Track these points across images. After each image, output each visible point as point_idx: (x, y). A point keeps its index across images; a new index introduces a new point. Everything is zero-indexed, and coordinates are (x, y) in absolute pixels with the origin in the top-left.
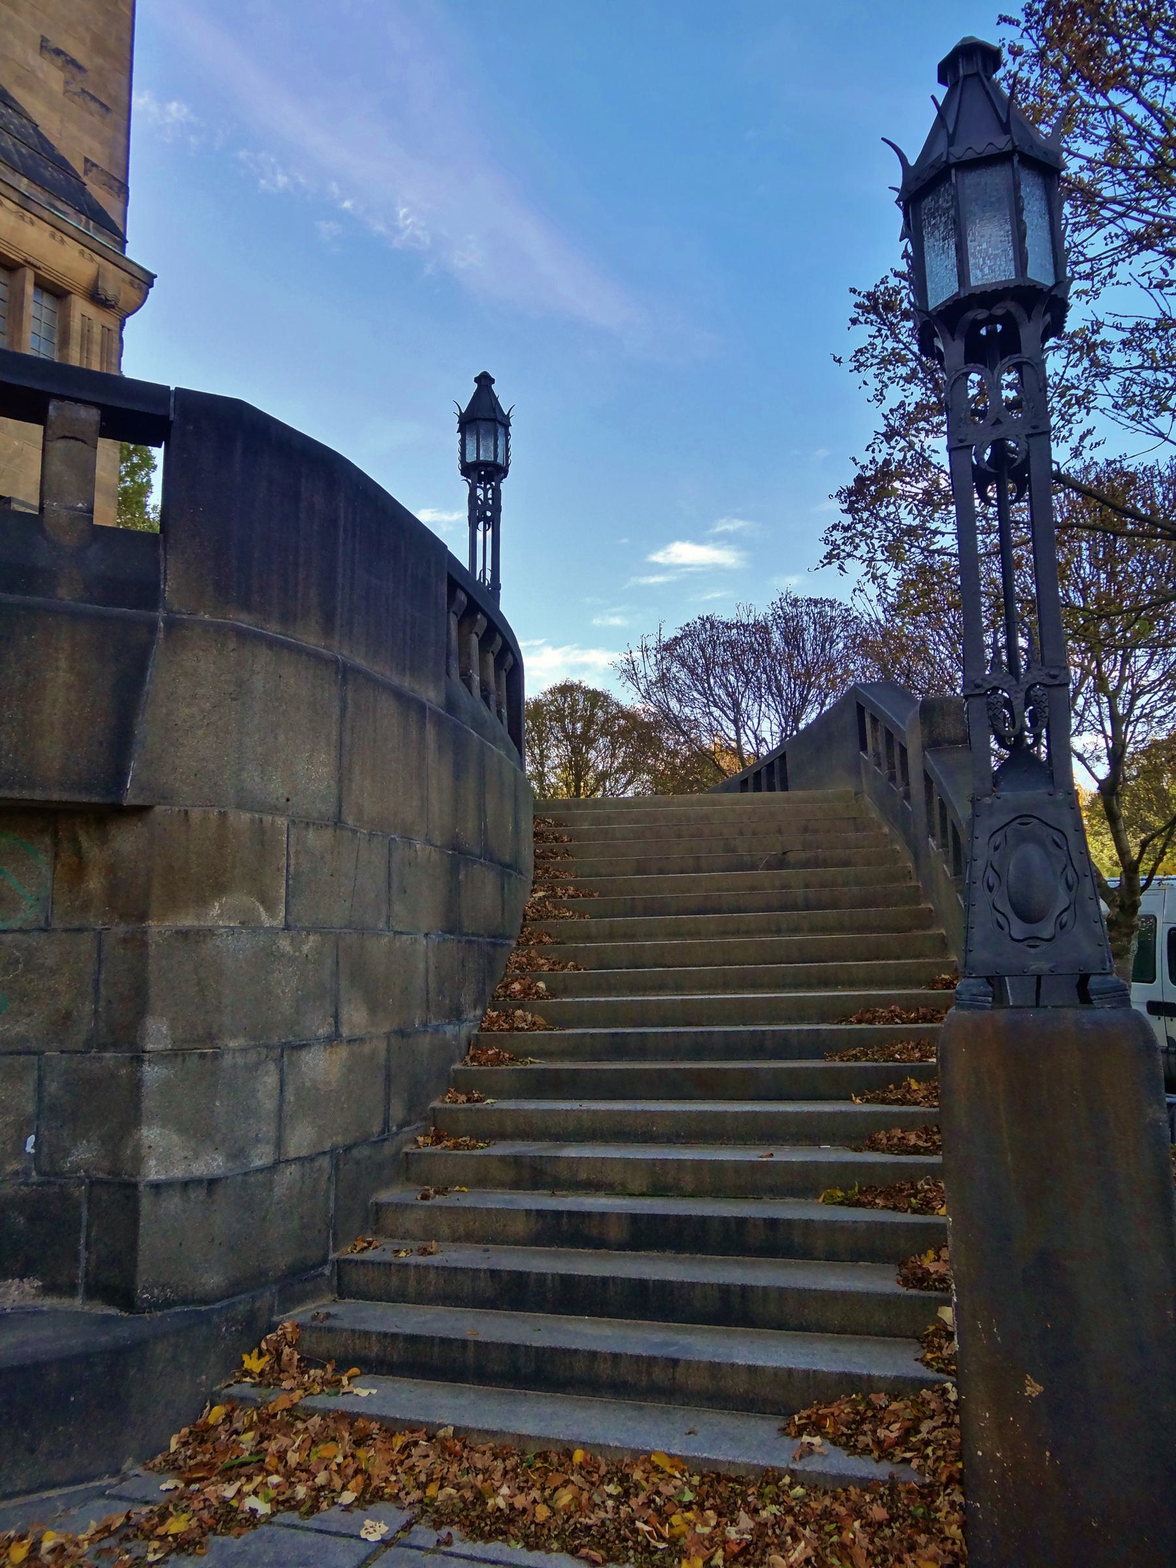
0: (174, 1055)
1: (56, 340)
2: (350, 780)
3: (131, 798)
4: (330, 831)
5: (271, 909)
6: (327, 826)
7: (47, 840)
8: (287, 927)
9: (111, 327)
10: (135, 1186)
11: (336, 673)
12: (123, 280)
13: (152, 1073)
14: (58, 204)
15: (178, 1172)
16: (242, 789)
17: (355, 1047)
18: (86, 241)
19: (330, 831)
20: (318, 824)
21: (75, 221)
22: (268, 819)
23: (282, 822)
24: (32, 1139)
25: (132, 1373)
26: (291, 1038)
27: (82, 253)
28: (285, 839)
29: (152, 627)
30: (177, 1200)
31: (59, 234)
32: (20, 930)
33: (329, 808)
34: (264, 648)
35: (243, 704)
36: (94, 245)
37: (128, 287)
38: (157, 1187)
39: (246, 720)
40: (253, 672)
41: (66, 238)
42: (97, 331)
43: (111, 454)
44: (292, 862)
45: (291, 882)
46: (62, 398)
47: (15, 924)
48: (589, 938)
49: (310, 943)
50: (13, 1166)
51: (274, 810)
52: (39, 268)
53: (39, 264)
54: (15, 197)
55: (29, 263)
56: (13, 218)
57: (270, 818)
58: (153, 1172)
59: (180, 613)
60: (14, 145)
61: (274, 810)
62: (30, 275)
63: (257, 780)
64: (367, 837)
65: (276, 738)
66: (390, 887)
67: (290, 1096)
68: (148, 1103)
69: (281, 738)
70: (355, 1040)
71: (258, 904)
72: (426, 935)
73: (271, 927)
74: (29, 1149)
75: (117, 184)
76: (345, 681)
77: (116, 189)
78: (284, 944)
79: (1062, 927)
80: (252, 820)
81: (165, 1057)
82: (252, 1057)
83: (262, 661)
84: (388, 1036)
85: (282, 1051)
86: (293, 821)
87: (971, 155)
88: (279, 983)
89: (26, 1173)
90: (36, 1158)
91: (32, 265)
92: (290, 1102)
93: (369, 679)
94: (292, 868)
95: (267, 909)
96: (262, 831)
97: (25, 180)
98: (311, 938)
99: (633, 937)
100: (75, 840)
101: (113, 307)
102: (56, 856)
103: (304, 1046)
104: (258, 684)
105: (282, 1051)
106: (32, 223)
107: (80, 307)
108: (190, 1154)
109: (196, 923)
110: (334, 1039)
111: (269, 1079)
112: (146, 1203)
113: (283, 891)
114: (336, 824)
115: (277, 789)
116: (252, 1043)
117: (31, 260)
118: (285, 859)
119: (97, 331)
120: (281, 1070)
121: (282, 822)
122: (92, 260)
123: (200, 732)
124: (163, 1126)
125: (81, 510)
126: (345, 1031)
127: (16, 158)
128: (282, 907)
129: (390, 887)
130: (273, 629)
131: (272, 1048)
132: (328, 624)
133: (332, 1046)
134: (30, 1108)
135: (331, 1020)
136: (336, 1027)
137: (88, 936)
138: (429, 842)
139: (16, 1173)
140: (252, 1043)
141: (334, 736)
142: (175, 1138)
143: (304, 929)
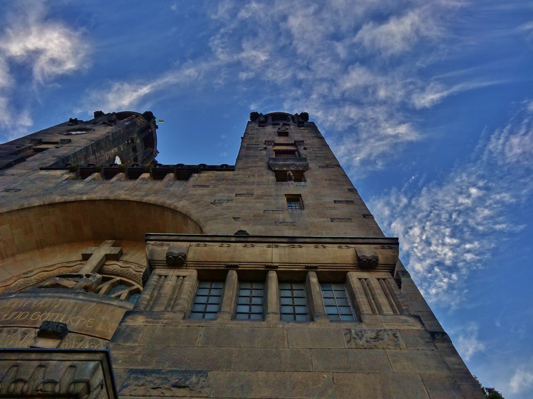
1: (350, 304)
43: (429, 353)
56: (287, 249)
106: (301, 247)
119: (374, 283)
122: (349, 248)
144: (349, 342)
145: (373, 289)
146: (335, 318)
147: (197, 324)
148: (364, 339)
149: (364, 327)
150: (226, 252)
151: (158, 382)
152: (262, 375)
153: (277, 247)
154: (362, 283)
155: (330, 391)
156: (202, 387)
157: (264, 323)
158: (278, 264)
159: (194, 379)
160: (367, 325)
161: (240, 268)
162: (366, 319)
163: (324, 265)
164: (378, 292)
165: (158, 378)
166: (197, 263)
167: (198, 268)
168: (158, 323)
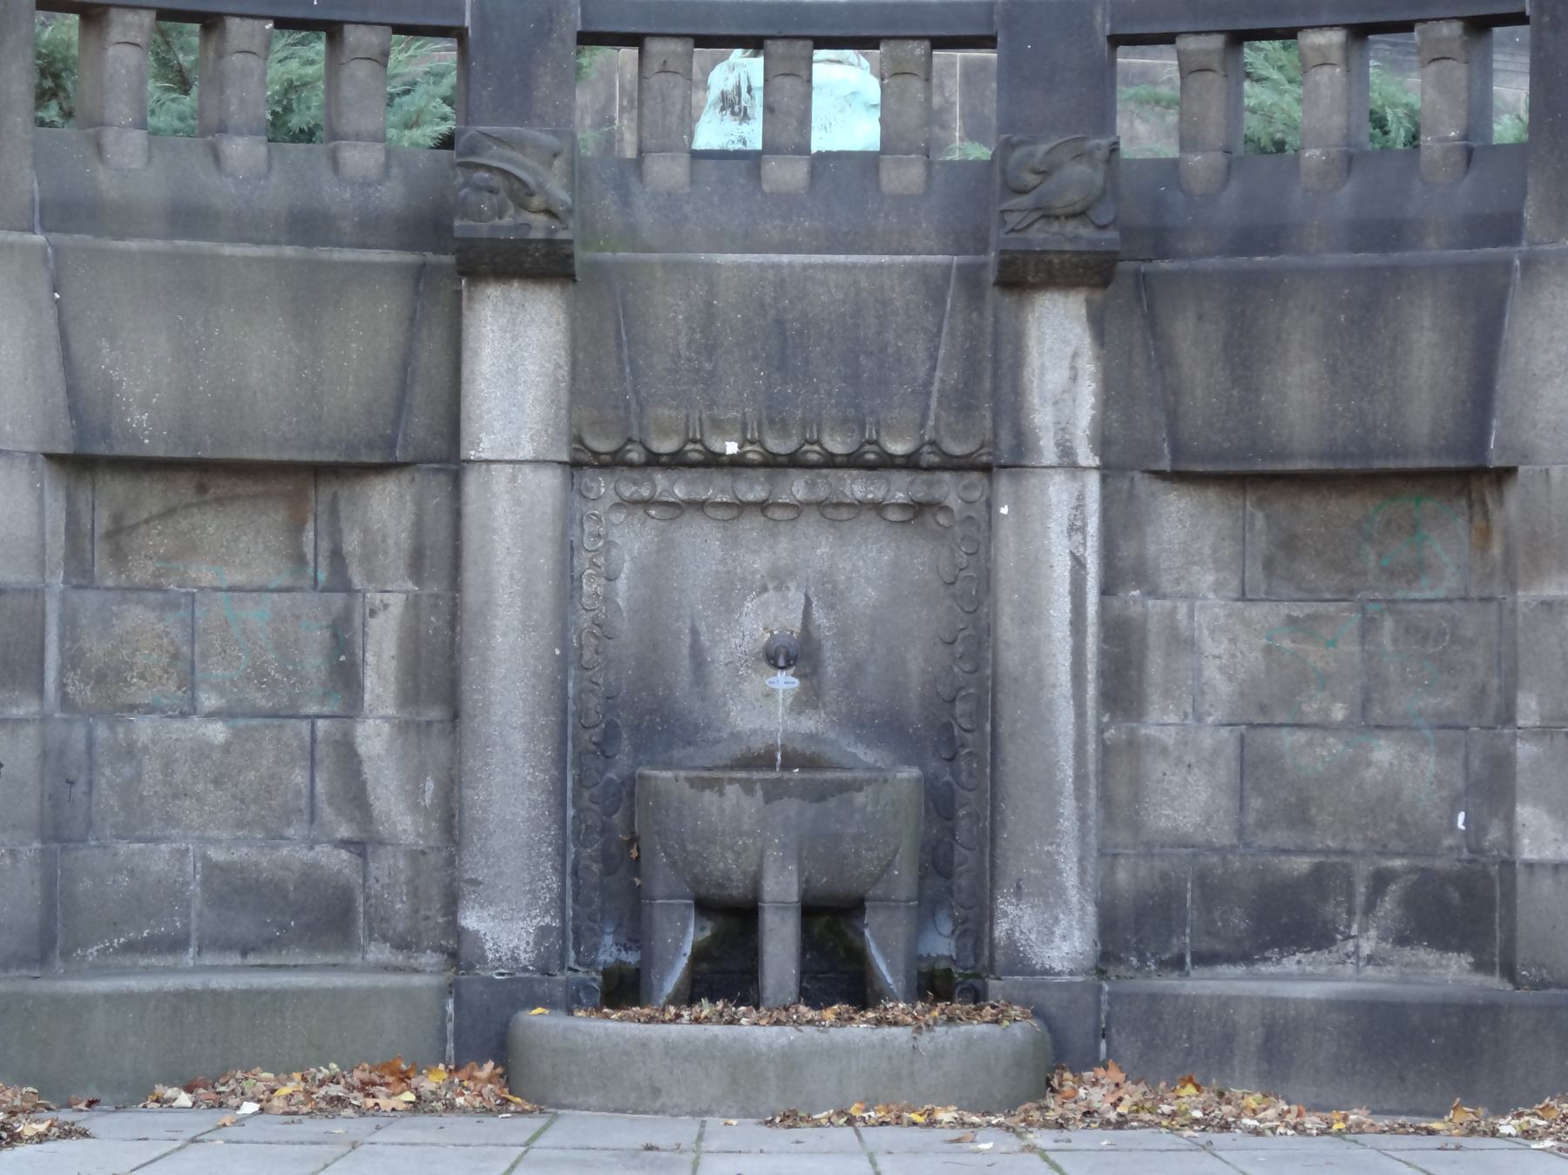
0: (1543, 732)
3: (1495, 461)
7: (1464, 502)
10: (1513, 863)
13: (1525, 751)
15: (1549, 854)
24: (1461, 817)
25: (1483, 1030)
29: (1507, 267)
30: (1549, 881)
32: (1447, 600)
38: (1530, 866)
46: (1424, 21)
47: (1441, 593)
50: (1448, 842)
58: (1528, 851)
59: (1542, 243)
68: (1521, 781)
74: (1460, 825)
81: (1536, 734)
89: (1459, 848)
90: (1465, 834)
100: (1483, 503)
102: (1471, 519)
108: (1559, 836)
109: (1559, 593)
112: (1522, 879)
123: (1558, 381)
124: (1535, 806)
125: (1454, 139)
134: (1460, 784)
137: (1494, 606)
139: (1451, 849)
142: (1545, 818)
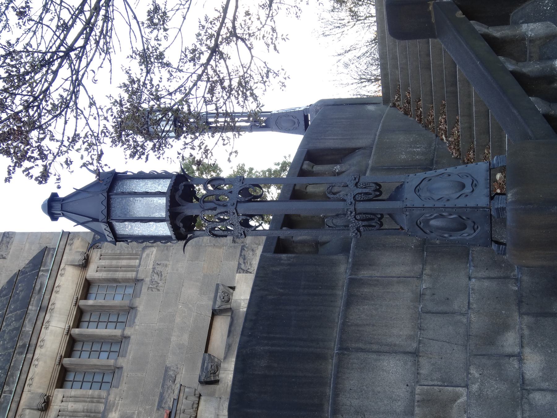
1: (115, 285)
2: (395, 345)
4: (421, 359)
5: (457, 396)
6: (418, 361)
8: (467, 386)
9: (99, 254)
11: (344, 354)
12: (70, 250)
14: (37, 288)
16: (405, 412)
17: (525, 341)
18: (54, 273)
19: (421, 359)
20: (417, 365)
21: (44, 279)
22: (417, 397)
23: (418, 389)
26: (519, 384)
27: (62, 275)
28: (426, 387)
31: (55, 289)
33: (409, 358)
34: (340, 399)
35: (366, 411)
36: (56, 268)
37: (74, 247)
39: (373, 410)
40: (351, 405)
41: (56, 285)
42: (103, 263)
43: (174, 251)
44: (436, 383)
45: (446, 384)
48: (470, 128)
49: (473, 371)
51: (413, 393)
52: (77, 298)
53: (75, 299)
54: (42, 315)
55: (76, 304)
56: (54, 315)
57: (417, 396)
60: (11, 312)
61: (413, 393)
62: (82, 303)
63: (399, 403)
64: (422, 332)
65: (379, 392)
66: (446, 313)
67: (545, 385)
69: (379, 389)
70: (522, 342)
71: (456, 404)
72: (470, 278)
73: (467, 395)
75: (5, 239)
76: (347, 349)
77: (8, 240)
78: (475, 387)
79: (468, 219)
80: (419, 406)
82: (526, 407)
83: (344, 399)
84: (521, 314)
85: (524, 389)
86: (417, 382)
87: (108, 229)
88: (493, 391)
91: (76, 302)
92: (549, 385)
93: (343, 331)
94: (439, 383)
95: (459, 397)
96: (423, 400)
97: (30, 307)
98: (472, 372)
99: (470, 105)
101: (88, 256)
103: (523, 376)
104: (355, 402)
105: (524, 389)
106: (54, 304)
107: (92, 273)
110: (520, 357)
111: (538, 398)
113: (450, 389)
114: (417, 356)
115: (402, 392)
116: (520, 407)
117: (74, 302)
118: (435, 388)
119: (103, 263)
120: (533, 390)
121: (418, 389)
122: (64, 269)
126: (517, 350)
127: (19, 312)
128: (457, 389)
129: (446, 313)
130: (329, 392)
131: (522, 394)
132: (321, 357)
133: (524, 359)
135: (511, 359)
136: (513, 356)
138: (420, 277)
140: (520, 407)
141: (374, 356)
143: (467, 376)
144: (159, 290)
145: (111, 265)
146: (136, 295)
147: (125, 378)
148: (159, 282)
149: (148, 280)
150: (45, 362)
151: (169, 392)
152: (173, 339)
153: (48, 322)
154: (101, 271)
155: (190, 306)
156: (177, 368)
157: (132, 337)
158: (67, 325)
159: (171, 373)
160: (146, 277)
161: (63, 355)
162: (141, 276)
163: (76, 292)
164: (114, 262)
165: (167, 391)
166: (49, 387)
167: (54, 387)
168: (118, 403)
